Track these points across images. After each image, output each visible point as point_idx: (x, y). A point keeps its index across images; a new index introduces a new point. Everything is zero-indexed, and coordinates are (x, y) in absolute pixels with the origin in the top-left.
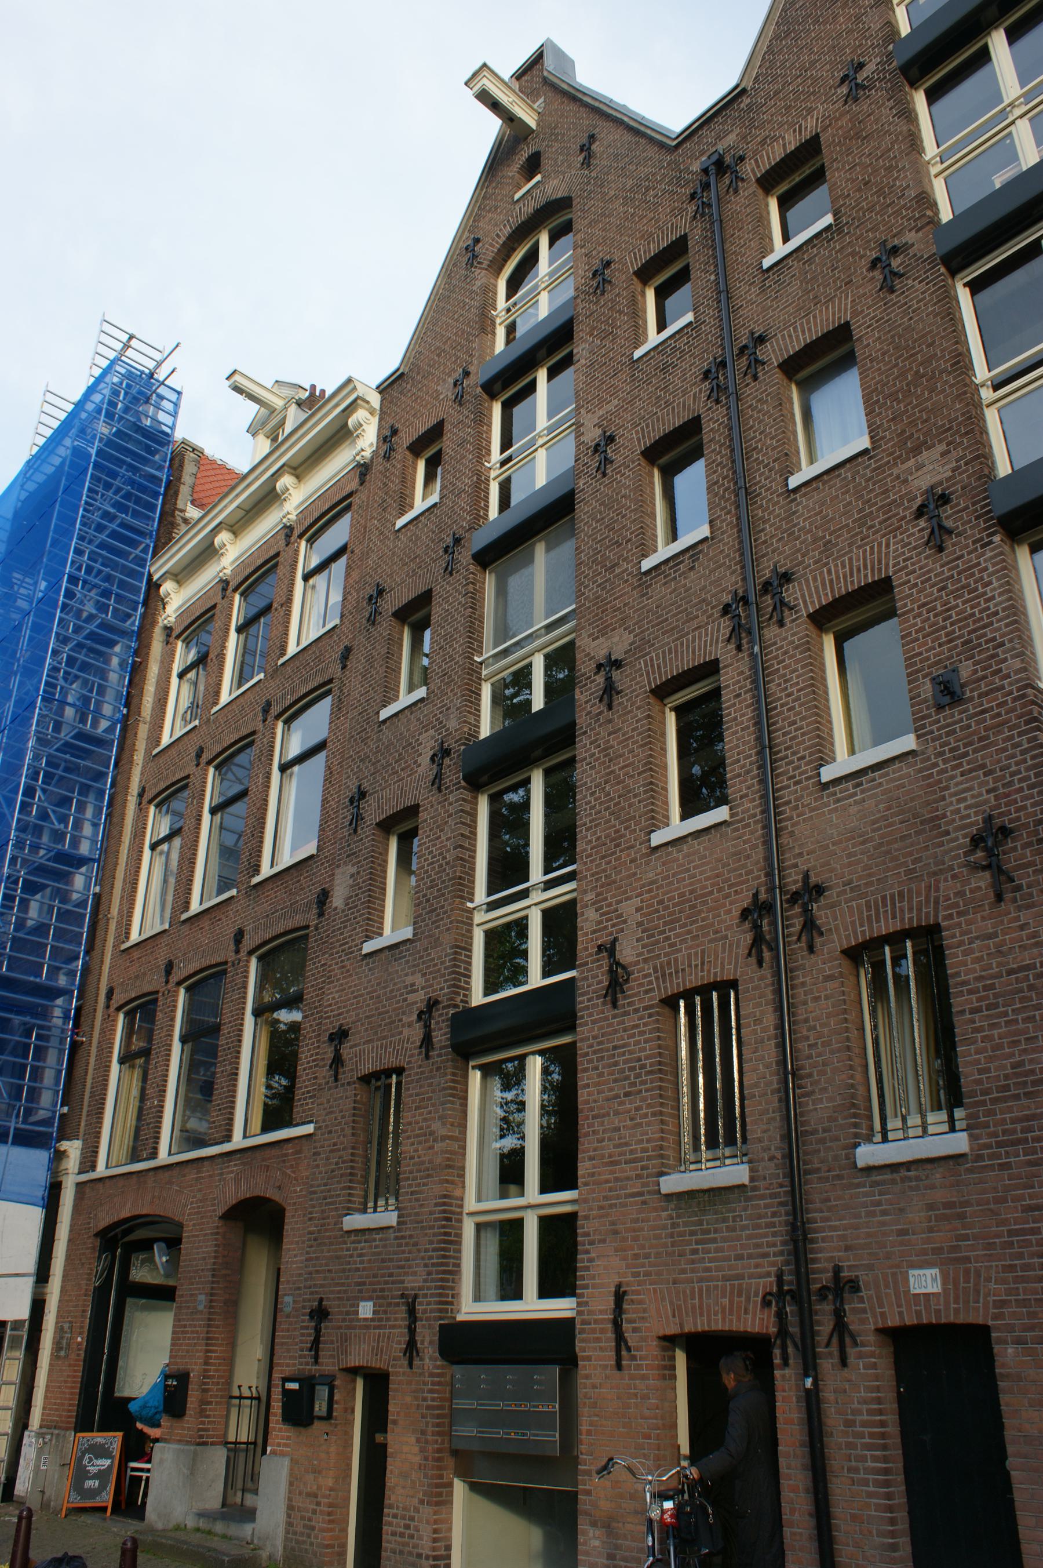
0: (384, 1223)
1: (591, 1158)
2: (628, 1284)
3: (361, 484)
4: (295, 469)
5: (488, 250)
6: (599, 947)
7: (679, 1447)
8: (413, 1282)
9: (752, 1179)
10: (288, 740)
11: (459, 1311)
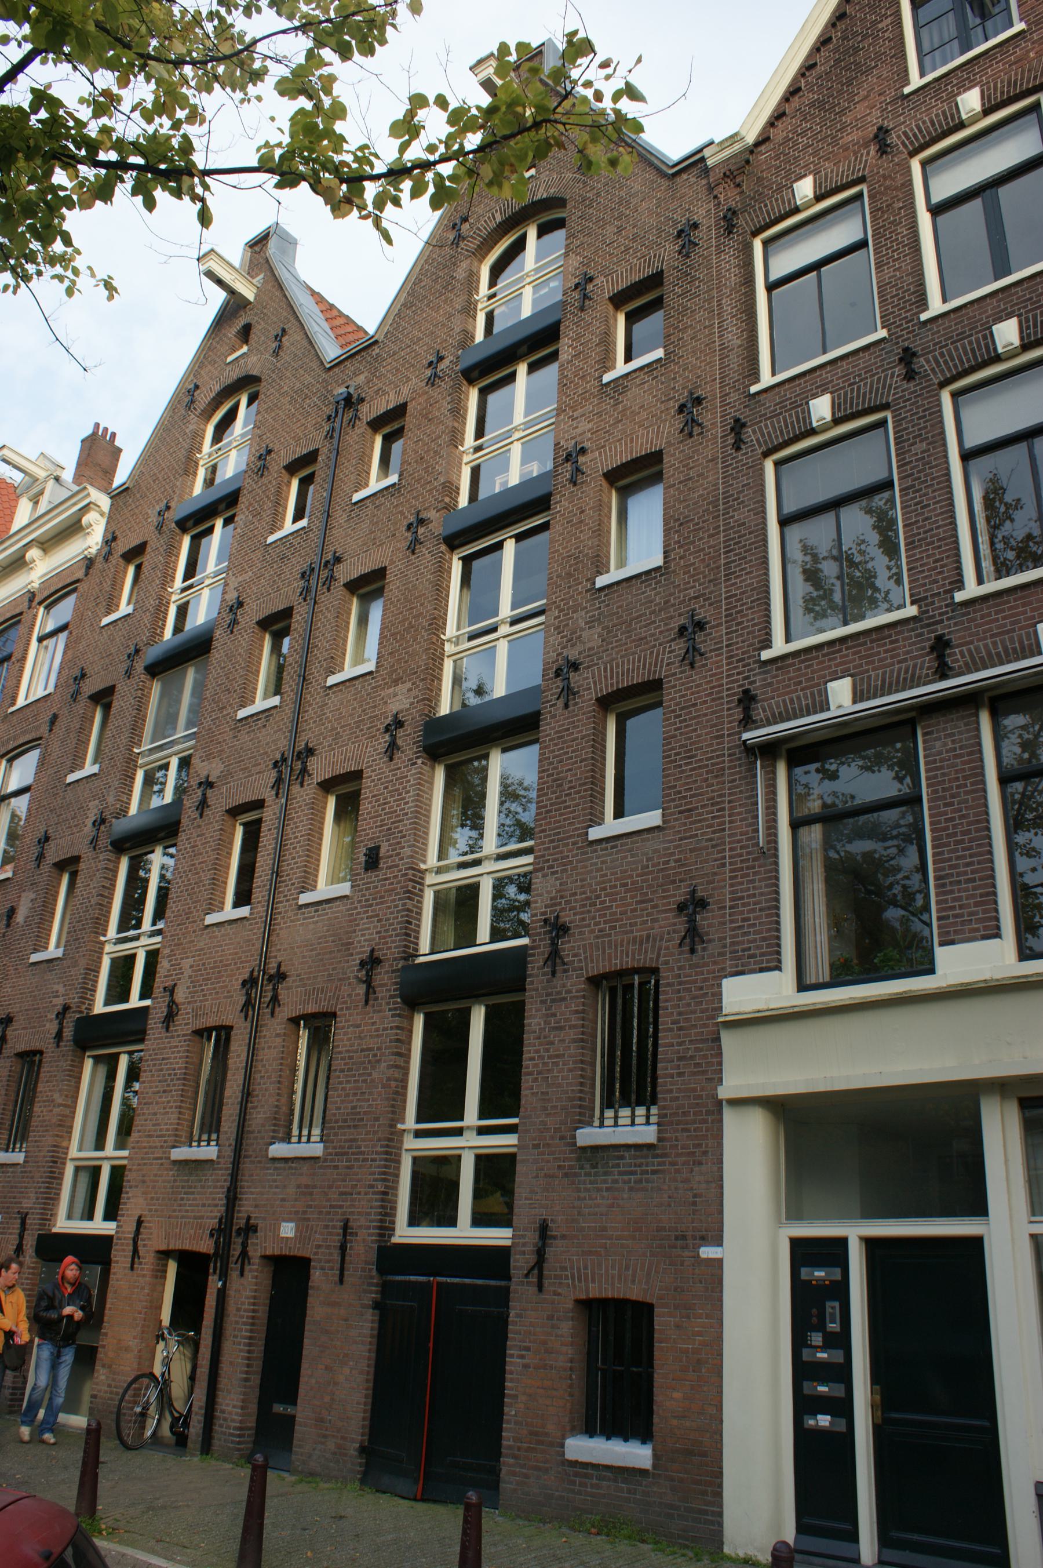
0: (15, 1161)
1: (139, 1131)
2: (145, 1216)
3: (86, 575)
4: (42, 544)
5: (204, 398)
6: (165, 988)
7: (161, 1321)
8: (27, 1204)
9: (218, 1157)
10: (10, 774)
11: (54, 1226)
